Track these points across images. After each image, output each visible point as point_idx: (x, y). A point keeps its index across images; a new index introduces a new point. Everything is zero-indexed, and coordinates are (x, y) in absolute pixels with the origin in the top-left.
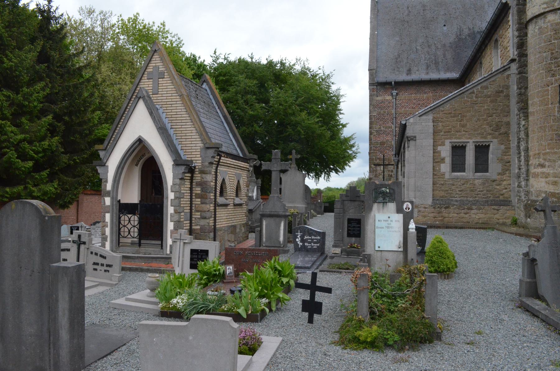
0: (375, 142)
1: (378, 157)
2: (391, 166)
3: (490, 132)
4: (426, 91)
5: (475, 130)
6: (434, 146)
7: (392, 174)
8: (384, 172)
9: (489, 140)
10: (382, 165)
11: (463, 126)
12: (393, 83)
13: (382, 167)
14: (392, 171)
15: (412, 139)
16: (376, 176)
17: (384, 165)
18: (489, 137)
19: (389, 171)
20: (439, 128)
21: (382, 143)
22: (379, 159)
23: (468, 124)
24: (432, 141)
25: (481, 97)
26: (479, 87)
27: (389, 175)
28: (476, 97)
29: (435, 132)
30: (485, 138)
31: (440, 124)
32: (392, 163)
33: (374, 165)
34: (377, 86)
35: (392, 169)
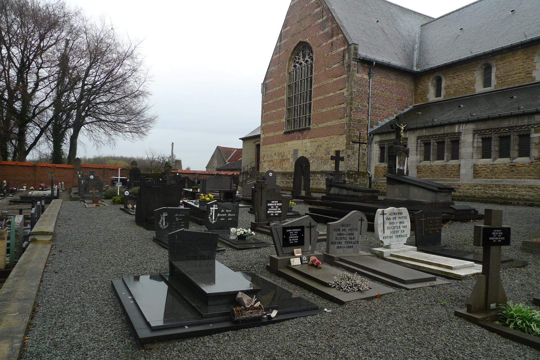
0: (354, 119)
1: (356, 134)
2: (364, 145)
4: (392, 77)
7: (365, 152)
8: (359, 151)
10: (358, 143)
12: (374, 63)
13: (358, 144)
14: (365, 150)
16: (353, 154)
17: (359, 143)
19: (363, 149)
21: (360, 121)
22: (356, 136)
27: (363, 153)
32: (366, 142)
33: (352, 142)
34: (357, 62)
35: (365, 148)
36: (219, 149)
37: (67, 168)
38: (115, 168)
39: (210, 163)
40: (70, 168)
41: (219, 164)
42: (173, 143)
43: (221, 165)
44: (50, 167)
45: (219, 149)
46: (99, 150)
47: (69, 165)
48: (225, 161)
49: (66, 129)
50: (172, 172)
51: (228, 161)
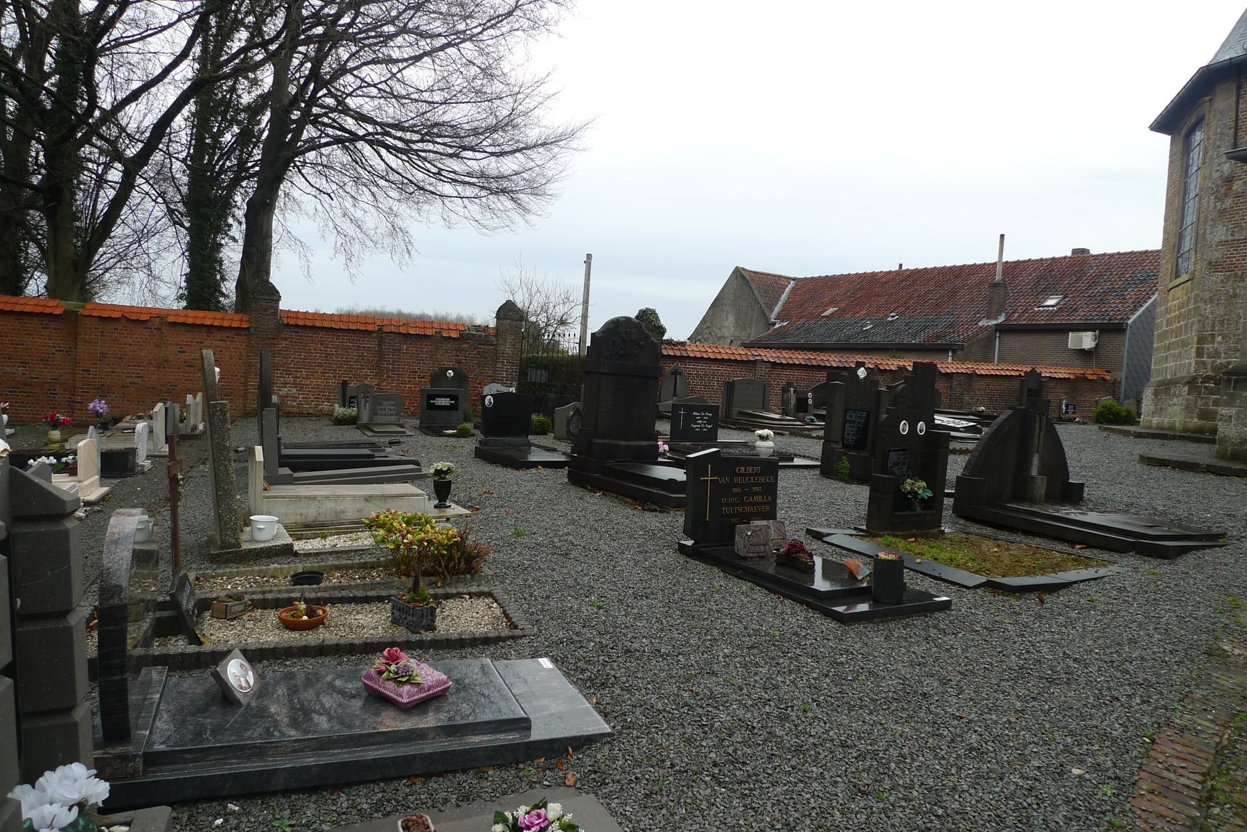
36: (744, 277)
37: (220, 328)
38: (429, 332)
39: (708, 324)
40: (230, 328)
41: (744, 329)
42: (589, 256)
43: (754, 334)
44: (138, 321)
45: (741, 278)
46: (353, 271)
47: (200, 314)
48: (766, 319)
49: (235, 183)
50: (665, 352)
51: (780, 317)
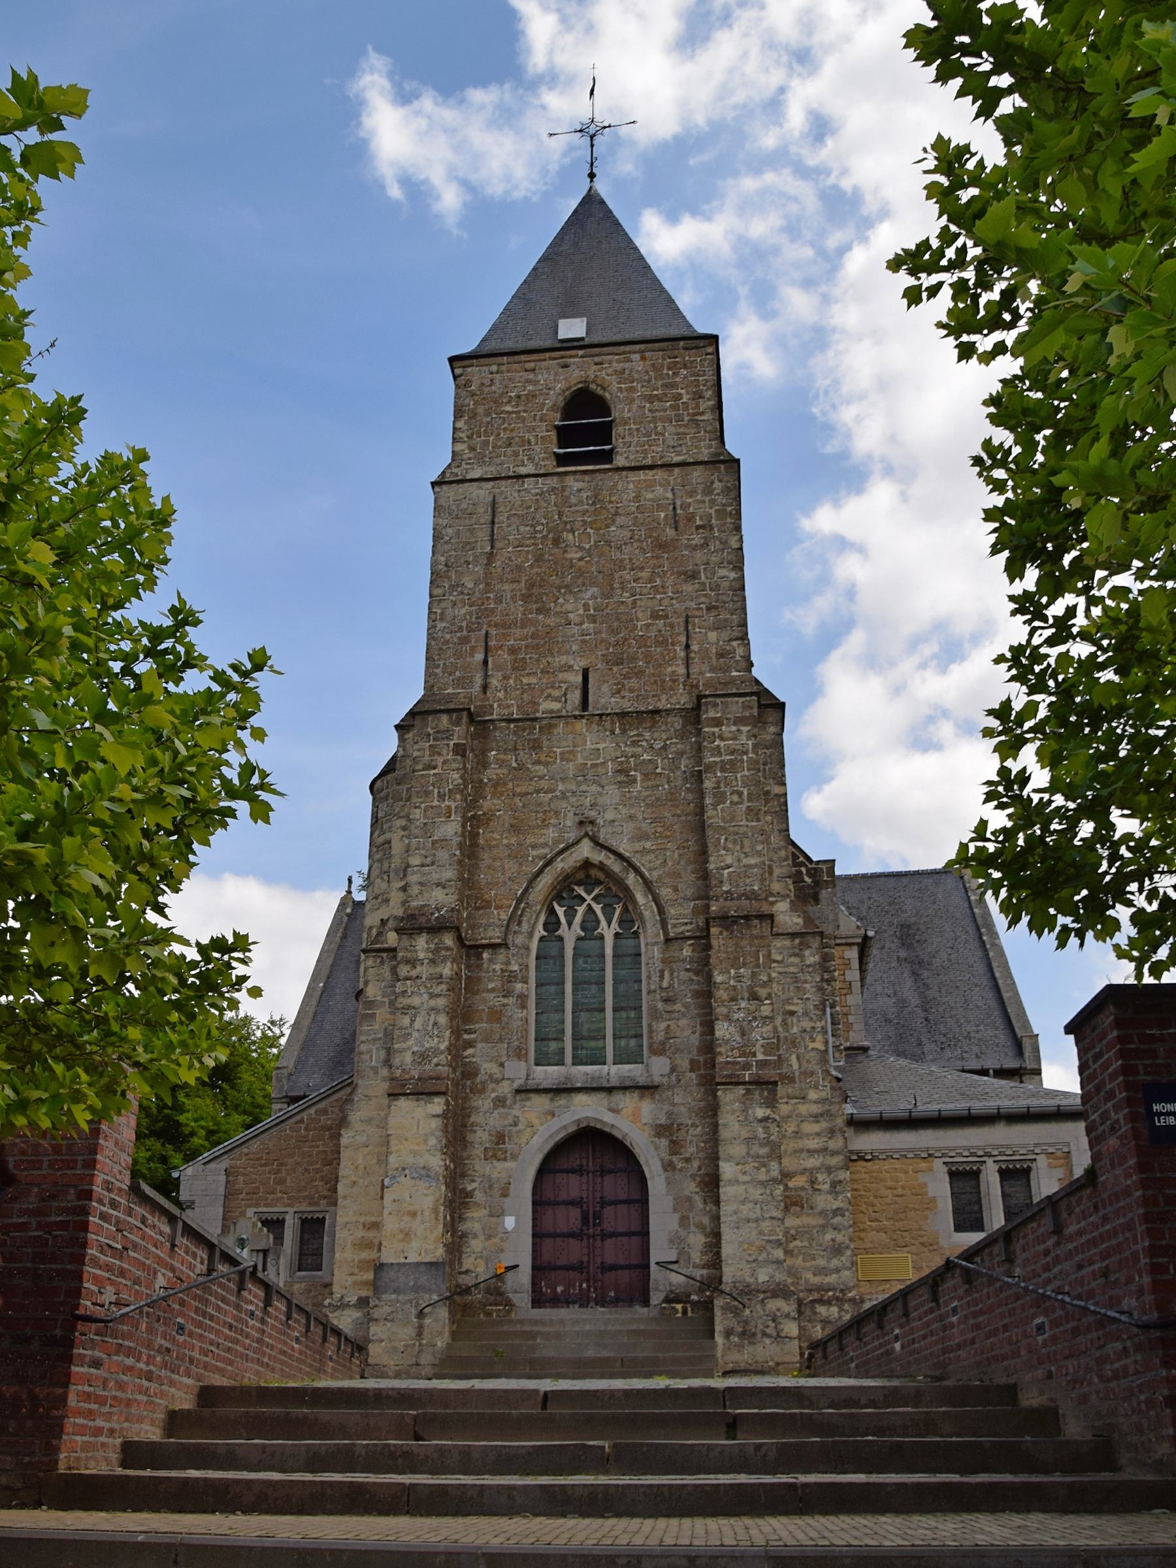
3: (325, 1193)
5: (299, 1191)
6: (224, 1219)
9: (321, 1208)
11: (281, 1182)
15: (188, 1207)
18: (323, 1202)
20: (237, 1187)
23: (288, 1180)
24: (221, 1210)
25: (315, 1129)
26: (312, 1111)
28: (306, 1129)
29: (230, 1194)
30: (316, 1204)
31: (241, 1178)
